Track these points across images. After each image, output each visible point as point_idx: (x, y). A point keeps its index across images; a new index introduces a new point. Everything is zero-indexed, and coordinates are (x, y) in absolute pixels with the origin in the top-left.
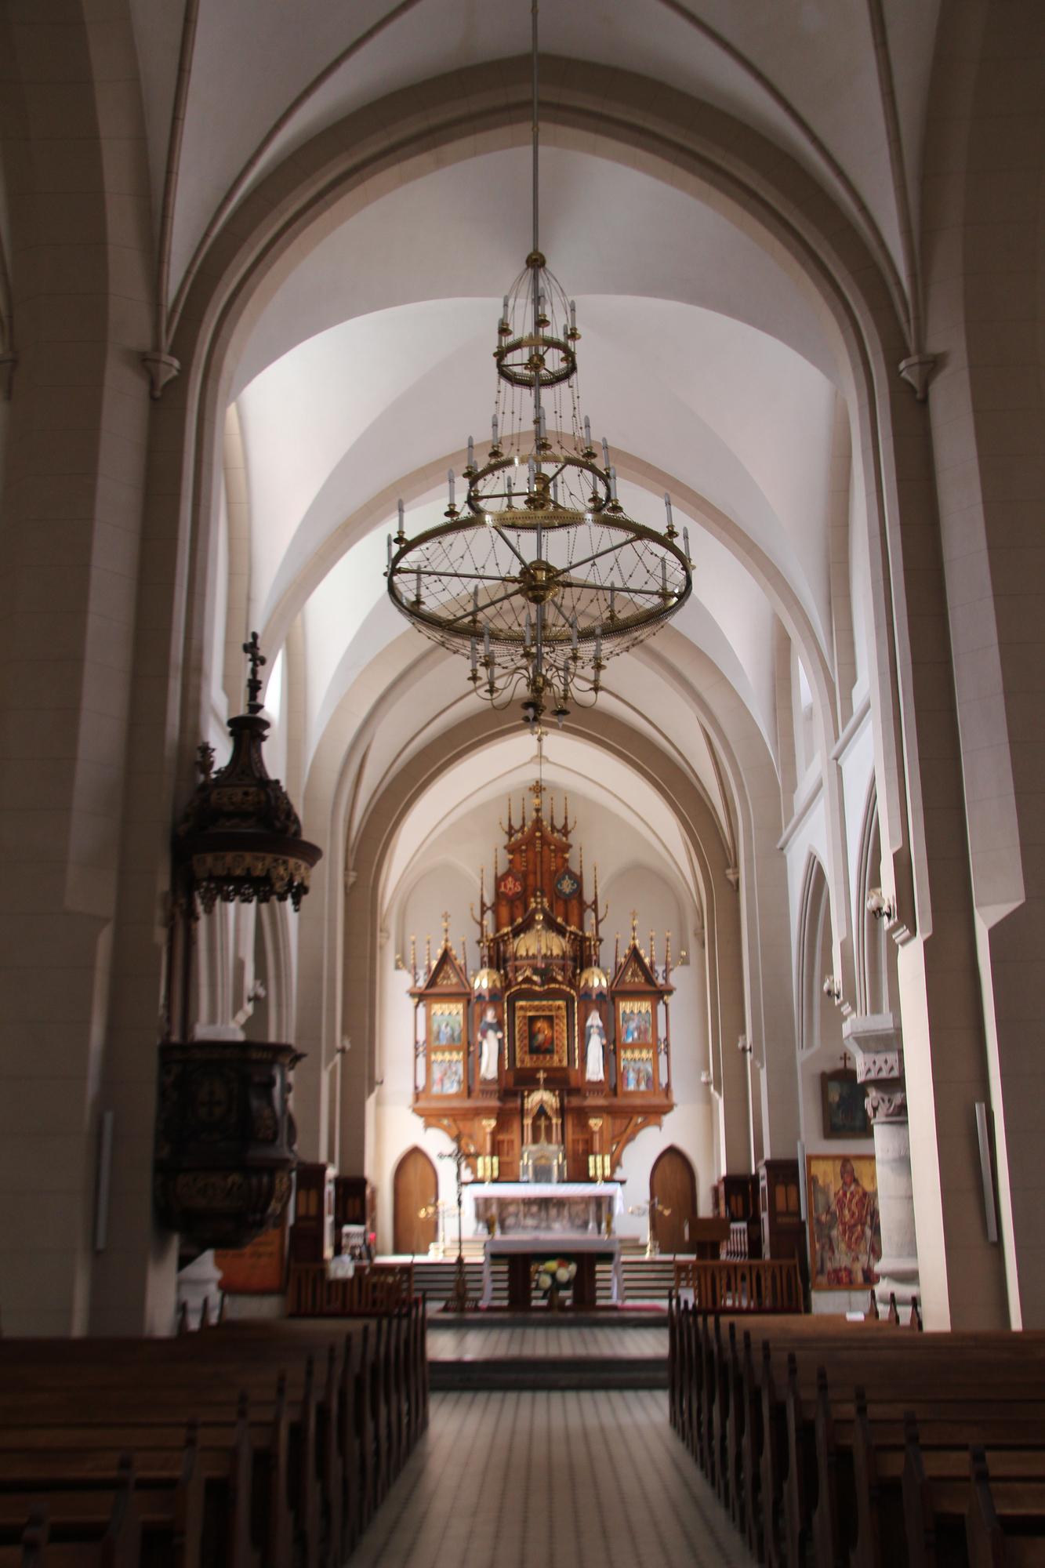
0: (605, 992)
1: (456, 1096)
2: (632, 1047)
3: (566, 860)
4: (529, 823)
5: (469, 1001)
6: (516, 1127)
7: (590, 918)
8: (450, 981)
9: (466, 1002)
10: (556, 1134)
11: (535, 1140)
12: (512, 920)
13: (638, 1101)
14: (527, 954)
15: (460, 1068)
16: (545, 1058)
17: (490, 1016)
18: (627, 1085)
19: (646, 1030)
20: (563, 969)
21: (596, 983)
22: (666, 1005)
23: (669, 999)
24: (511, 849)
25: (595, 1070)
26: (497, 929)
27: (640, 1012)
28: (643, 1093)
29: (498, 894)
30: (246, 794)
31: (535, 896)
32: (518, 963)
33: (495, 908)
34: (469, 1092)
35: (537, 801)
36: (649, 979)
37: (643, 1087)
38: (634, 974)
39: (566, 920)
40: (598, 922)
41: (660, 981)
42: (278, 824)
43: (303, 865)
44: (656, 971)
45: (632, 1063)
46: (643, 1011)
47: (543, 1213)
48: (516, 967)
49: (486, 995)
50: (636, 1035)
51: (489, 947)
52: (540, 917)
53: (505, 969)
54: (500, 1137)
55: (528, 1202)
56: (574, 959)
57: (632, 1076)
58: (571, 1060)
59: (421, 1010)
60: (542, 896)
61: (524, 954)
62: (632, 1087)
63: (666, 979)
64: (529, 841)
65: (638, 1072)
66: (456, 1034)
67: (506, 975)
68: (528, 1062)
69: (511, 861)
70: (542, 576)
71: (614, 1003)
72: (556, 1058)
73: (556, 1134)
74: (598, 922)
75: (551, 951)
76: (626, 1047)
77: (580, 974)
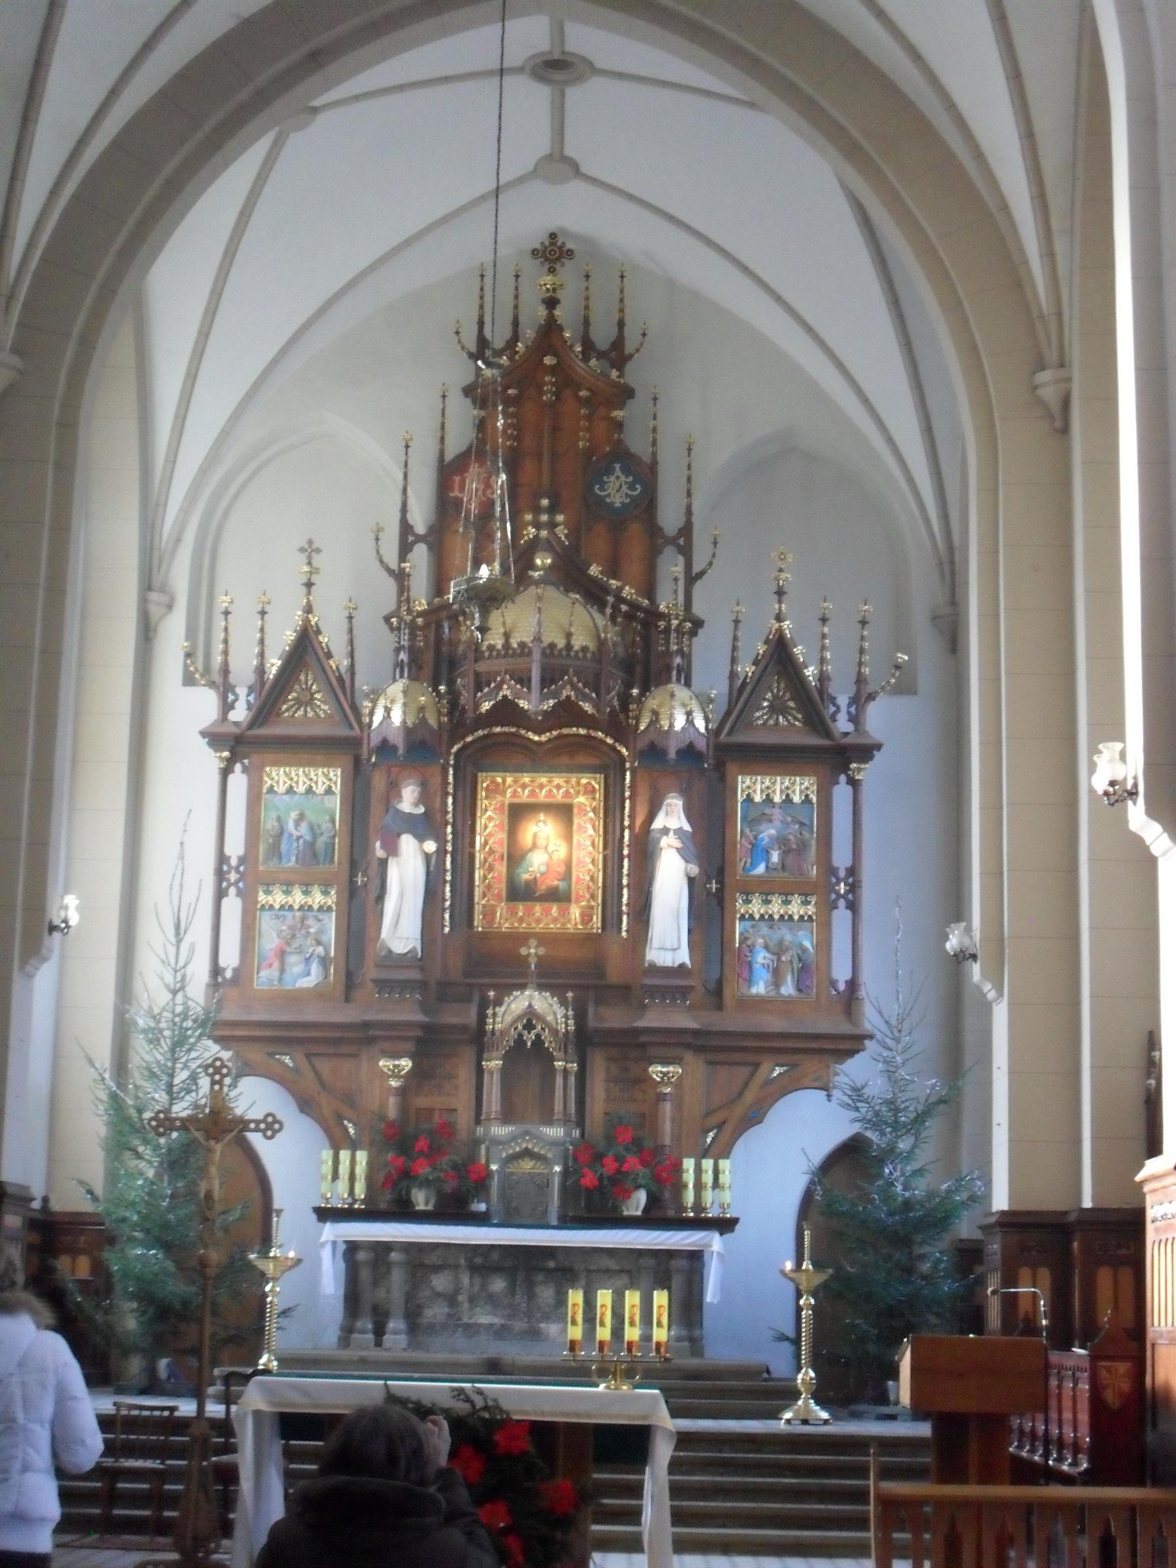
0: (701, 745)
2: (766, 888)
5: (357, 761)
6: (464, 1075)
9: (348, 761)
13: (775, 1024)
14: (507, 645)
16: (547, 912)
18: (750, 982)
19: (803, 846)
22: (854, 783)
23: (866, 772)
27: (788, 800)
28: (788, 1002)
32: (482, 667)
36: (816, 721)
37: (788, 989)
38: (777, 708)
41: (843, 724)
44: (833, 700)
45: (764, 928)
46: (797, 799)
48: (477, 675)
49: (398, 740)
50: (775, 857)
53: (451, 683)
57: (761, 957)
62: (760, 988)
63: (855, 719)
65: (778, 950)
66: (321, 841)
71: (722, 778)
72: (575, 912)
75: (569, 636)
77: (639, 700)
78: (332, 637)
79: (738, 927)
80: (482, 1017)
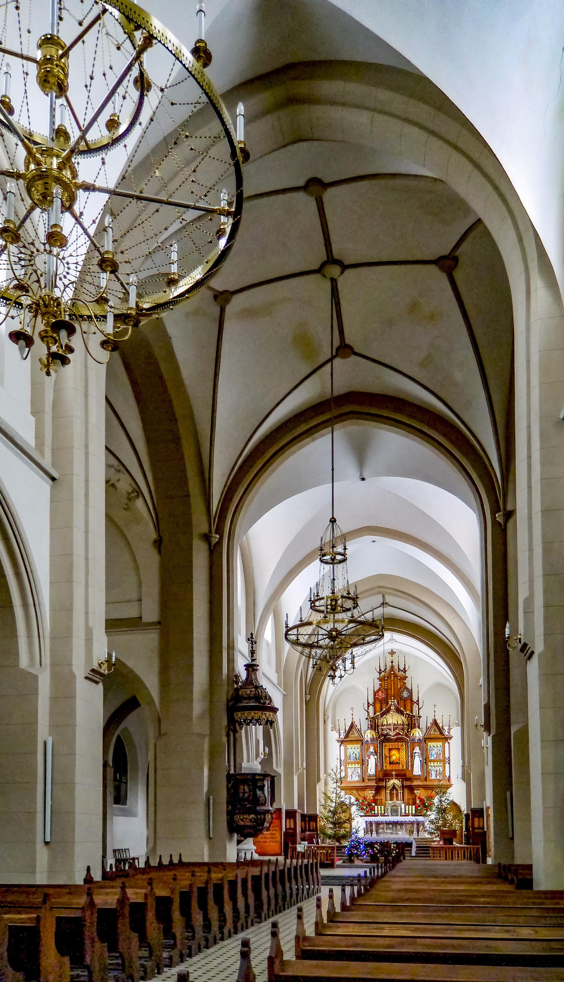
1: (358, 782)
3: (405, 683)
4: (388, 668)
6: (383, 793)
7: (415, 707)
8: (355, 735)
10: (400, 796)
11: (391, 799)
12: (381, 709)
13: (436, 783)
15: (359, 771)
17: (372, 749)
20: (403, 729)
21: (417, 735)
24: (380, 679)
25: (417, 770)
26: (375, 714)
29: (375, 699)
30: (251, 691)
31: (391, 699)
33: (374, 704)
34: (363, 781)
35: (392, 658)
39: (405, 709)
40: (419, 709)
42: (262, 701)
43: (271, 714)
47: (394, 828)
51: (371, 721)
52: (393, 708)
53: (378, 730)
54: (376, 798)
55: (388, 823)
56: (408, 725)
57: (433, 773)
58: (407, 768)
59: (342, 747)
60: (394, 699)
61: (386, 724)
62: (433, 777)
64: (389, 676)
67: (378, 733)
68: (389, 767)
69: (380, 685)
70: (334, 633)
73: (400, 796)
74: (419, 709)
76: (431, 761)
78: (357, 723)
79: (429, 768)
80: (386, 784)
